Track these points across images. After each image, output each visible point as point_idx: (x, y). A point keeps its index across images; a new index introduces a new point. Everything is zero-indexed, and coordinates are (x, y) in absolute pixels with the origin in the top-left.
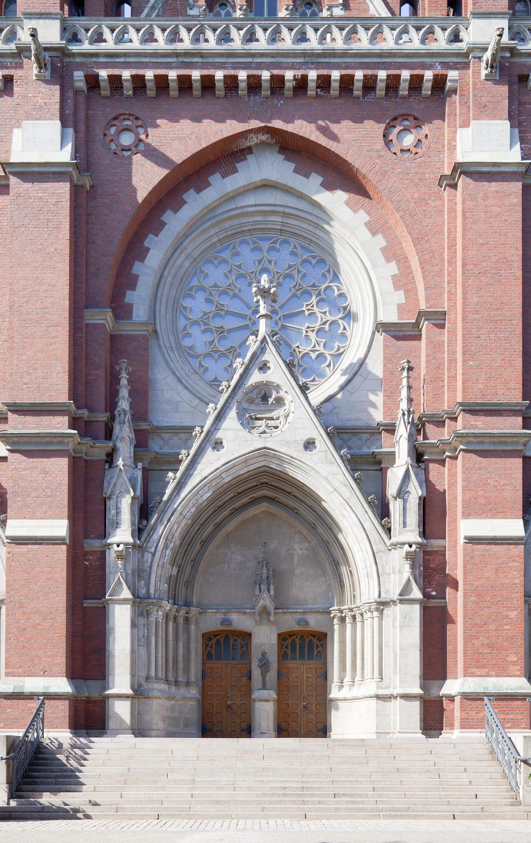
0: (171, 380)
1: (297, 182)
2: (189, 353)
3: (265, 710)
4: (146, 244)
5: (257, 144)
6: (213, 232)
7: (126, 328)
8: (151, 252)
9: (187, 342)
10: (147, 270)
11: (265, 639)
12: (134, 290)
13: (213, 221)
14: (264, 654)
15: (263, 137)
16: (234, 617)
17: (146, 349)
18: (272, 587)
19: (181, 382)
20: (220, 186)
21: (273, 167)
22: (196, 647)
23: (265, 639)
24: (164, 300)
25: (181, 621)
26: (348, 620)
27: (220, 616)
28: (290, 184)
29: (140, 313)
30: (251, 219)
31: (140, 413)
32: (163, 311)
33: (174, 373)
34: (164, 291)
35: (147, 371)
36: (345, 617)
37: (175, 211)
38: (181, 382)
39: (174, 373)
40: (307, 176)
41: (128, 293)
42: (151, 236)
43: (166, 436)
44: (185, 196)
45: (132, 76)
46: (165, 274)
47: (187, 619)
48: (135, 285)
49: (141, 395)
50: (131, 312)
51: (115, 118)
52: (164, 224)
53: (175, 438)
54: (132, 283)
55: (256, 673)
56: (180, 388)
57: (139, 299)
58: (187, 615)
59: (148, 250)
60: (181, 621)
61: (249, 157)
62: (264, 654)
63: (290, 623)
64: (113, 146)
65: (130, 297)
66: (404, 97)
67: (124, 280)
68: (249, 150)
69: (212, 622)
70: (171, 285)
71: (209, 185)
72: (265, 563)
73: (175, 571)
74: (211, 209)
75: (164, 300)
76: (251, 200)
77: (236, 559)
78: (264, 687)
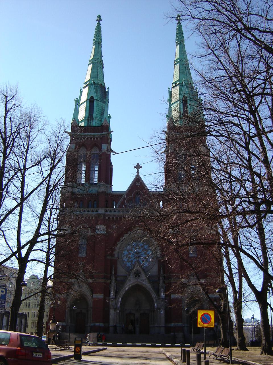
7: (114, 258)
23: (137, 315)
29: (116, 255)
57: (115, 253)
73: (121, 302)
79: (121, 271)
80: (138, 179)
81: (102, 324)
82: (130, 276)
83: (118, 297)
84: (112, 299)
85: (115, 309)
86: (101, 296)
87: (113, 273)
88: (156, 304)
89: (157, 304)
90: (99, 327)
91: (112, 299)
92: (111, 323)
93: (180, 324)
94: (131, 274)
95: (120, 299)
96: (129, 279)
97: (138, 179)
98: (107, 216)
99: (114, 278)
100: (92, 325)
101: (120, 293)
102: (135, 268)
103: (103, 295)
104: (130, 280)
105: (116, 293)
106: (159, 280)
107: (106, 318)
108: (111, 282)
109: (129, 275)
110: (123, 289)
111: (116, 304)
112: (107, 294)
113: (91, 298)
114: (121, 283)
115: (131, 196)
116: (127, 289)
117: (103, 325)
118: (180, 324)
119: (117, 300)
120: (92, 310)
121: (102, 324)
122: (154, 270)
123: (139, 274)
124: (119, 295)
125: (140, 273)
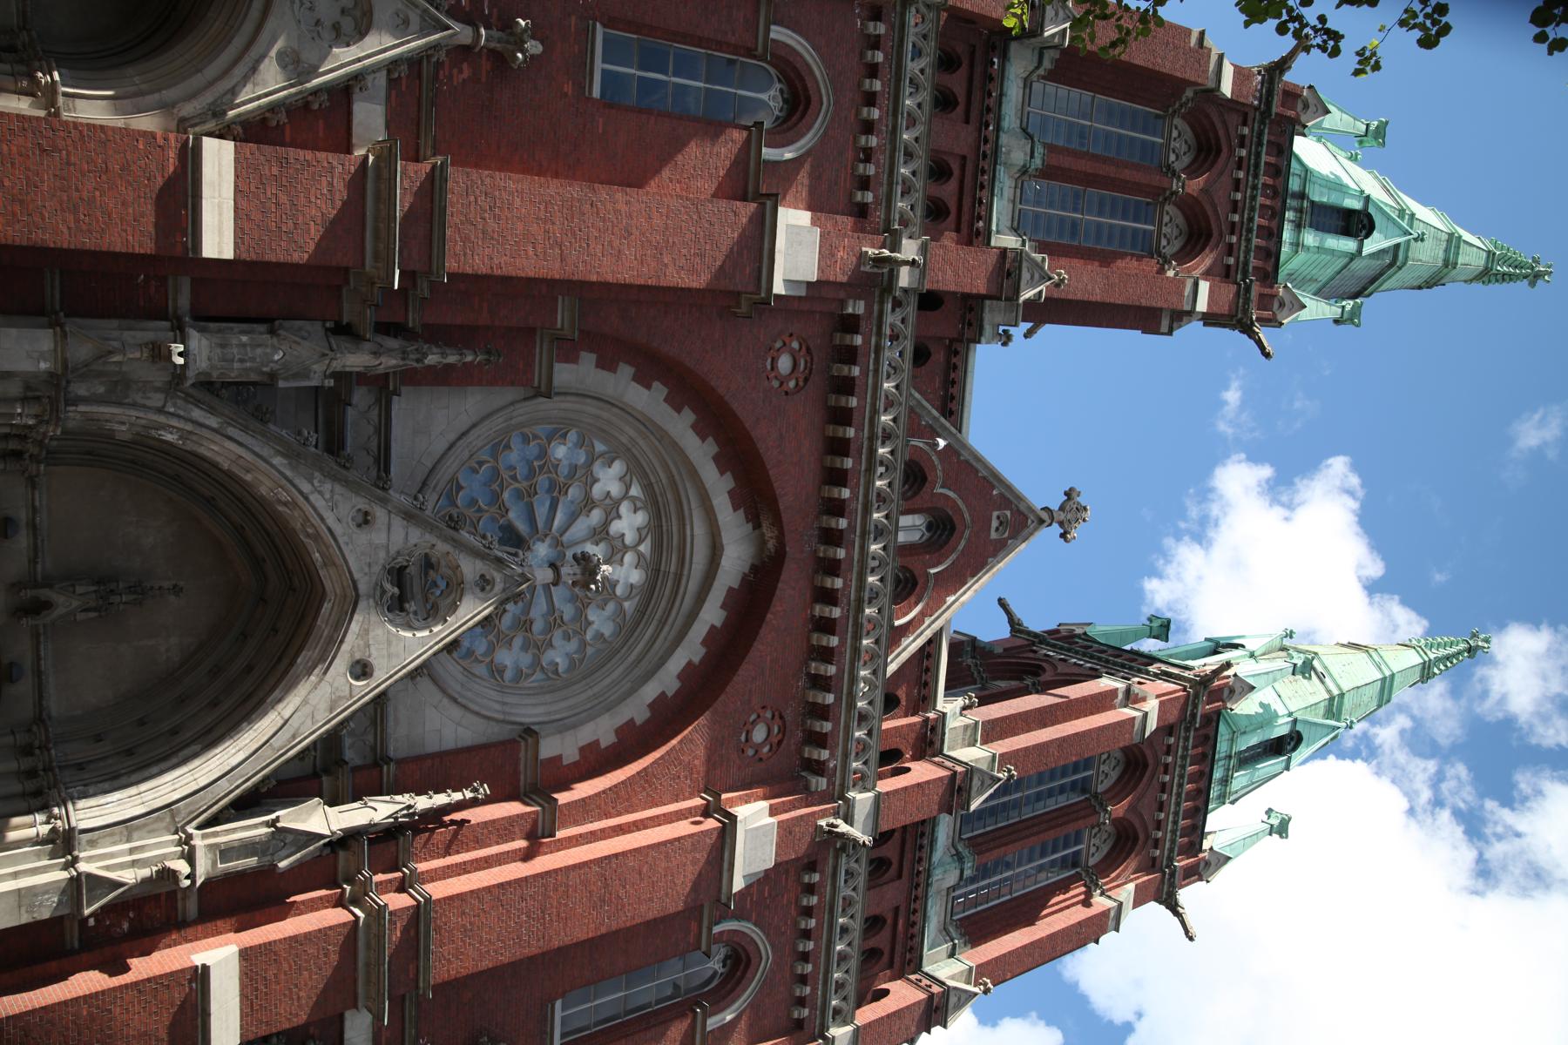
0: (464, 422)
2: (499, 446)
4: (656, 385)
5: (763, 535)
6: (662, 475)
8: (646, 392)
9: (516, 442)
10: (622, 385)
12: (597, 366)
13: (677, 477)
15: (771, 545)
17: (512, 384)
18: (93, 615)
19: (459, 438)
20: (719, 486)
21: (736, 559)
24: (577, 407)
25: (13, 445)
26: (27, 763)
28: (716, 584)
29: (564, 374)
30: (675, 529)
31: (415, 378)
32: (563, 406)
33: (474, 426)
34: (590, 408)
35: (480, 383)
36: (32, 754)
37: (694, 427)
38: (459, 438)
39: (474, 426)
40: (724, 606)
41: (593, 357)
42: (665, 391)
43: (374, 414)
44: (710, 439)
45: (853, 379)
46: (615, 410)
48: (603, 368)
49: (443, 377)
50: (567, 361)
51: (808, 349)
52: (679, 410)
53: (371, 429)
54: (607, 364)
56: (452, 437)
58: (26, 456)
59: (648, 387)
61: (750, 526)
64: (778, 345)
65: (588, 359)
66: (804, 723)
67: (610, 354)
68: (757, 526)
70: (598, 417)
71: (722, 473)
74: (694, 474)
75: (577, 407)
76: (699, 530)
79: (430, 425)
80: (1021, 520)
82: (398, 522)
83: (197, 414)
86: (218, 238)
87: (432, 359)
94: (416, 535)
96: (380, 513)
97: (1021, 520)
98: (869, 307)
99: (389, 362)
101: (231, 431)
103: (228, 254)
104: (365, 520)
108: (344, 331)
110: (278, 461)
111: (120, 389)
114: (333, 427)
115: (940, 482)
119: (157, 400)
124: (213, 422)
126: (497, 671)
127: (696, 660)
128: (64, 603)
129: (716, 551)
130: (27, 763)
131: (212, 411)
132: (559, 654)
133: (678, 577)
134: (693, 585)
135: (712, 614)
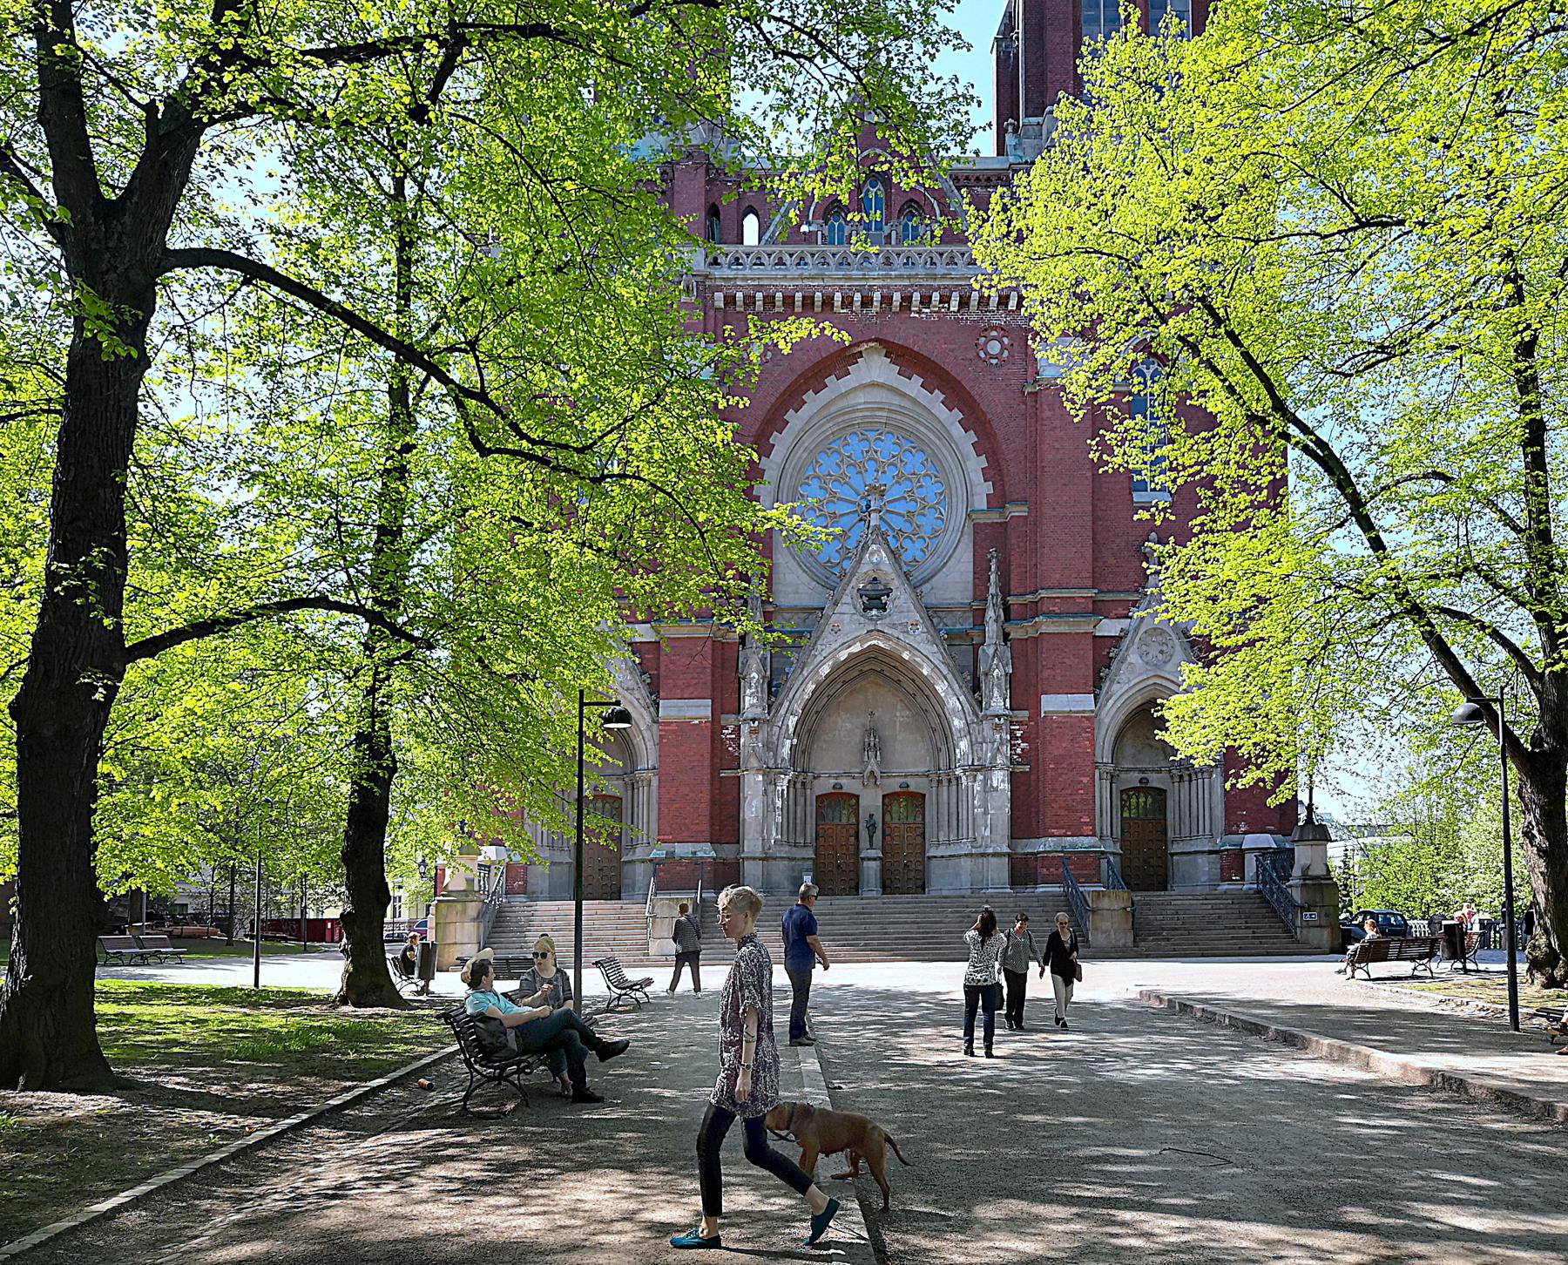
1: (901, 383)
3: (871, 869)
11: (871, 801)
14: (871, 816)
16: (843, 781)
22: (812, 809)
23: (871, 801)
25: (799, 786)
27: (833, 781)
34: (786, 481)
47: (803, 784)
55: (864, 833)
60: (799, 786)
62: (871, 816)
63: (893, 785)
68: (860, 354)
69: (824, 786)
72: (872, 731)
76: (861, 398)
77: (845, 727)
78: (871, 847)
81: (706, 851)
83: (782, 711)
84: (754, 720)
85: (770, 774)
88: (963, 745)
89: (972, 745)
90: (695, 862)
91: (754, 720)
92: (752, 844)
93: (1085, 842)
95: (792, 721)
100: (659, 853)
102: (865, 568)
105: (773, 689)
106: (980, 621)
107: (724, 821)
109: (836, 604)
111: (771, 747)
112: (726, 698)
113: (648, 719)
116: (825, 670)
117: (713, 854)
118: (1085, 842)
119: (776, 729)
120: (655, 782)
121: (706, 851)
122: (955, 579)
123: (884, 599)
124: (786, 704)
125: (888, 592)
126: (935, 534)
127: (942, 397)
128: (873, 765)
129: (873, 385)
130: (945, 783)
131: (781, 705)
132: (930, 489)
133: (890, 411)
134: (896, 400)
135: (914, 387)
